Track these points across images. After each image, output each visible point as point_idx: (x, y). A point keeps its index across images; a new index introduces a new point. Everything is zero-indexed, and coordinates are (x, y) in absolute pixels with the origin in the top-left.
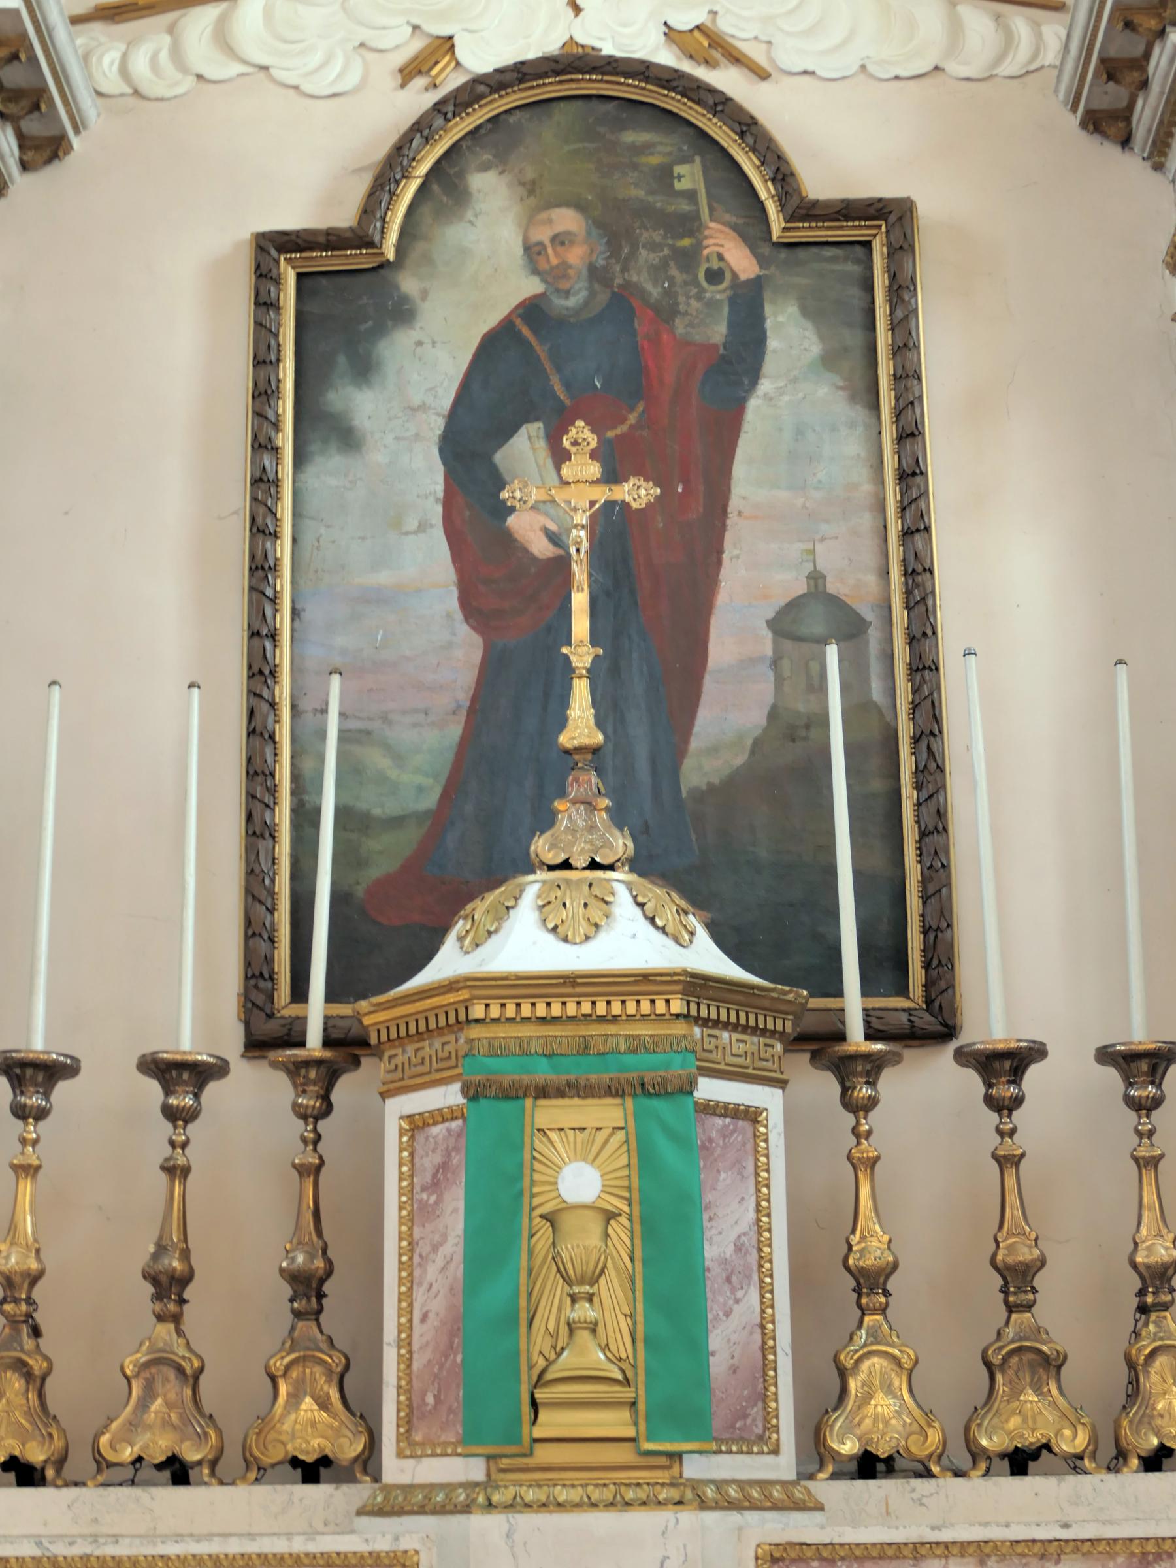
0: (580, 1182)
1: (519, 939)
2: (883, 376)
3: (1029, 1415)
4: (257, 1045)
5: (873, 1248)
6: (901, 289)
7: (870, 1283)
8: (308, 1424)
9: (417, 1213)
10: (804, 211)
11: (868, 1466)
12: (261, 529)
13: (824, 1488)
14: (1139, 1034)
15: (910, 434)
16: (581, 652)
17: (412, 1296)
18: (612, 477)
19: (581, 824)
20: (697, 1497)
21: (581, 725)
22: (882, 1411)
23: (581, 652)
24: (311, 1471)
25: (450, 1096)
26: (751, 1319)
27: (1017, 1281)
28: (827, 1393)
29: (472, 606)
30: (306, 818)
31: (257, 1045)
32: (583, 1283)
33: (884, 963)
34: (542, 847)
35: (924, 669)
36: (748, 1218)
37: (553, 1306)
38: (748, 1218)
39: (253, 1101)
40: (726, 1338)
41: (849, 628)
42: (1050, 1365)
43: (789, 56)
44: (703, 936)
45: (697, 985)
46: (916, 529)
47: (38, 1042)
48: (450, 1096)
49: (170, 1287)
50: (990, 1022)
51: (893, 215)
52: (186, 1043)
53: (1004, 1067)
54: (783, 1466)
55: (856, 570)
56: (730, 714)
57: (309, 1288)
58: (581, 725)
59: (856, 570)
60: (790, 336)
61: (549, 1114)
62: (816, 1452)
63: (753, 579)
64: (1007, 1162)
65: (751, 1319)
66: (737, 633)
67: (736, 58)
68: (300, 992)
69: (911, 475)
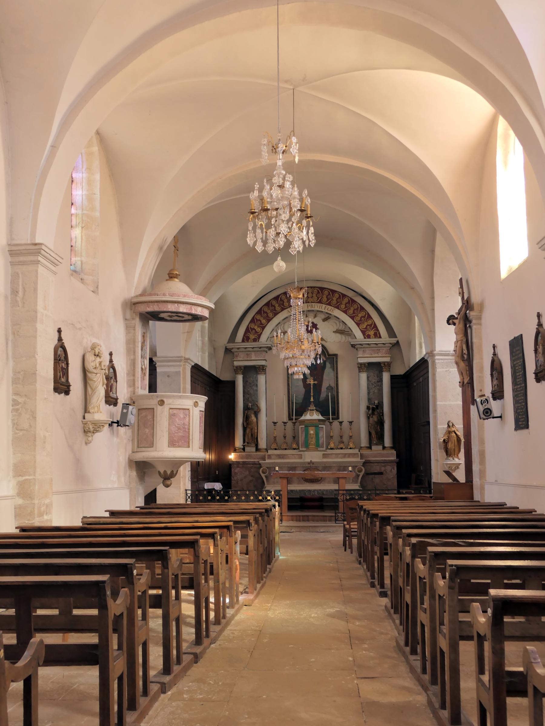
0: (312, 432)
1: (307, 417)
2: (335, 369)
3: (342, 445)
4: (289, 420)
5: (332, 434)
6: (337, 362)
7: (332, 437)
8: (294, 446)
9: (302, 433)
10: (329, 355)
11: (331, 449)
12: (288, 381)
13: (328, 450)
14: (350, 420)
15: (337, 373)
16: (312, 394)
17: (301, 438)
18: (314, 381)
19: (312, 407)
20: (319, 451)
21: (312, 400)
22: (332, 445)
23: (312, 394)
24: (294, 449)
25: (303, 426)
26: (323, 439)
27: (341, 437)
28: (328, 444)
29: (304, 387)
30: (293, 403)
31: (289, 420)
32: (312, 438)
33: (333, 414)
34: (310, 408)
35: (338, 392)
36: (323, 434)
37: (310, 440)
38: (323, 434)
39: (290, 424)
40: (321, 441)
41: (332, 388)
42: (343, 442)
43: (329, 340)
44: (320, 415)
45: (319, 420)
46: (337, 381)
47: (275, 421)
48: (303, 426)
49: (285, 437)
50: (340, 420)
51: (336, 355)
52: (285, 421)
53: (341, 423)
54: (324, 449)
55: (333, 385)
56: (323, 395)
57: (294, 437)
58: (312, 400)
59: (333, 385)
60: (328, 365)
61: (310, 428)
62: (327, 448)
63: (325, 385)
64: (341, 429)
65: (323, 439)
66: (324, 389)
67: (324, 340)
68: (293, 416)
69: (337, 377)
